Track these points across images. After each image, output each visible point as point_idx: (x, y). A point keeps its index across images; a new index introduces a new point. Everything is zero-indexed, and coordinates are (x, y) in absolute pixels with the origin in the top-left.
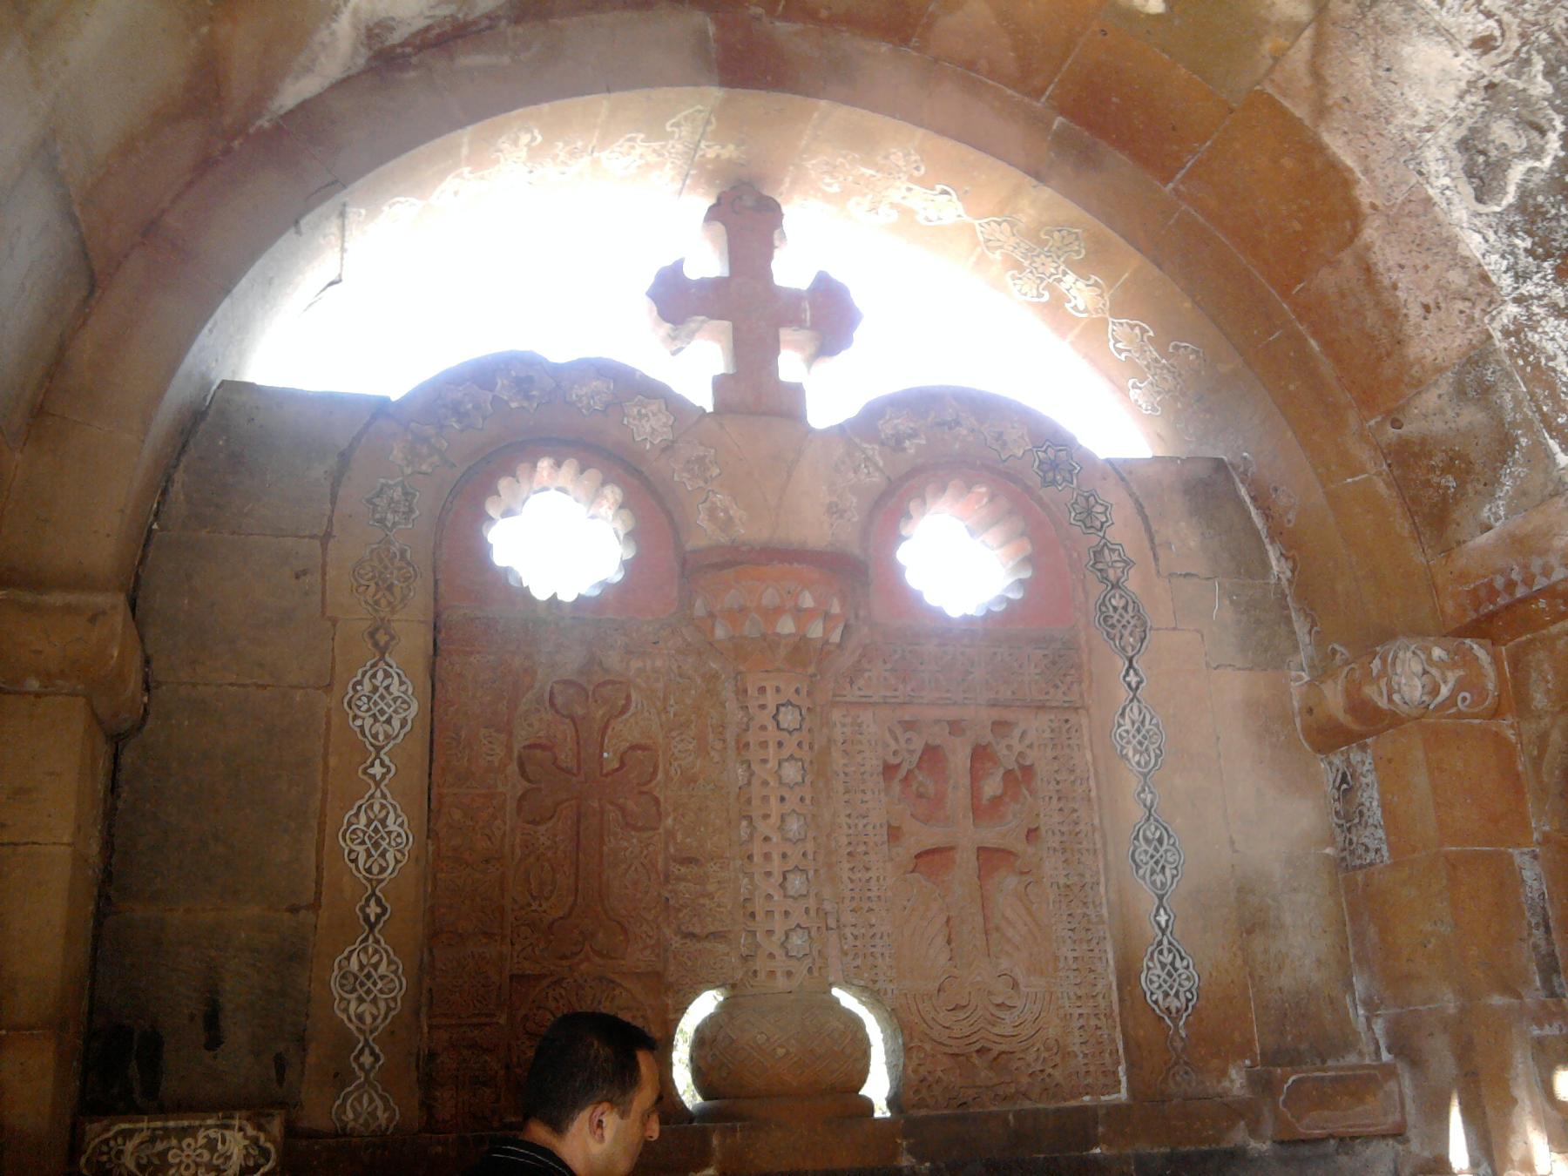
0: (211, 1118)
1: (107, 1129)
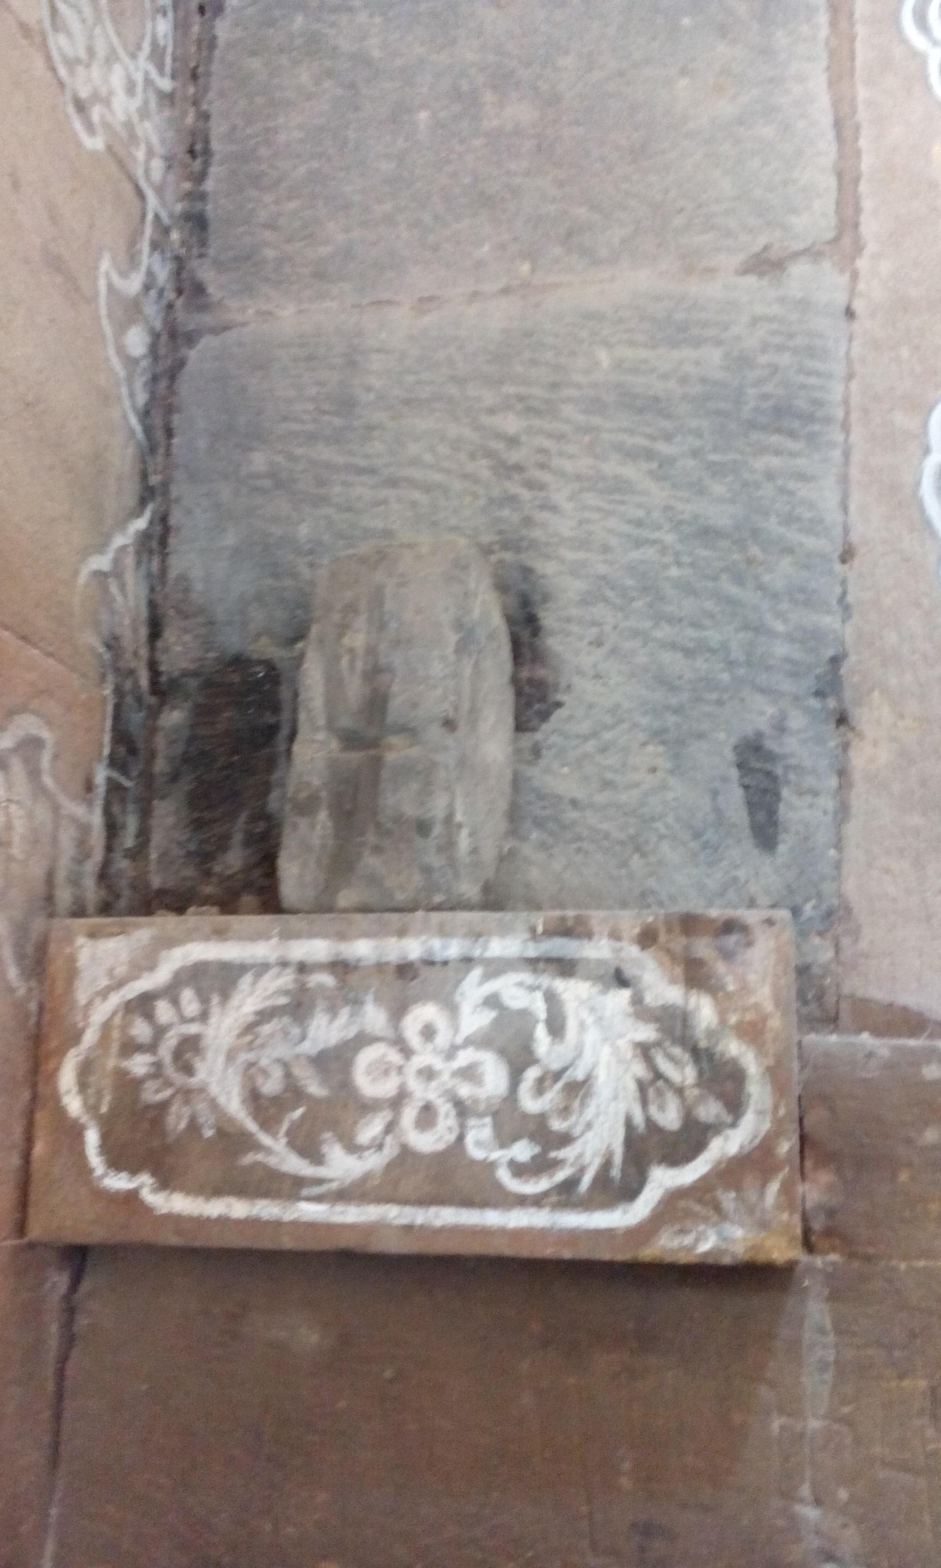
0: (504, 930)
1: (147, 962)
